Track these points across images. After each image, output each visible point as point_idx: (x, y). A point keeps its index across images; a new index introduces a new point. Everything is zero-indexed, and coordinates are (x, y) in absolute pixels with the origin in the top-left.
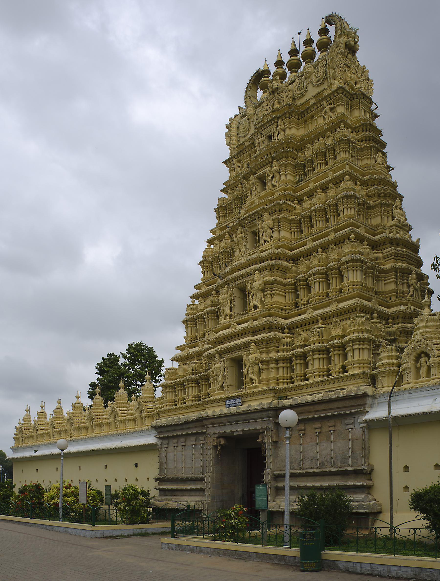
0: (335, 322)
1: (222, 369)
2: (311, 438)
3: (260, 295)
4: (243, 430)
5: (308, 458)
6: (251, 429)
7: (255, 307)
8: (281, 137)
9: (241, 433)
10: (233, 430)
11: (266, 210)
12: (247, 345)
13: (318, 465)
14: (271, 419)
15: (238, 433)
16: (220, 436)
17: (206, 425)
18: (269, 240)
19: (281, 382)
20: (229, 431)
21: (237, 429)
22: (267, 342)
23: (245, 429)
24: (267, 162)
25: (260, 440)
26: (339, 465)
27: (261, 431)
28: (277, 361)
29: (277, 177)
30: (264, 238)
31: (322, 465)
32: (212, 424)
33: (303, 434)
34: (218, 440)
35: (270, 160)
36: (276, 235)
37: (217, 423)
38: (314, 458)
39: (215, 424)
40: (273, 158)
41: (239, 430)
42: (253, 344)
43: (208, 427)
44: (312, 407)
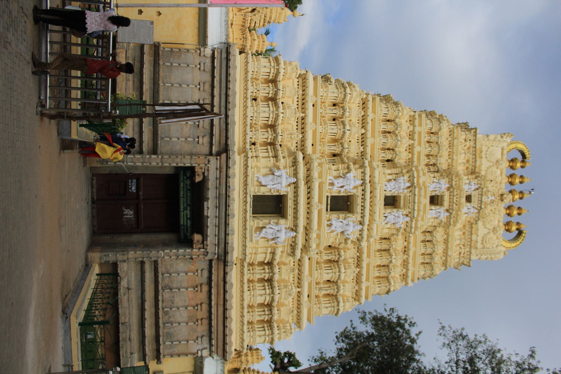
0: (292, 311)
1: (278, 187)
2: (193, 299)
3: (340, 230)
4: (208, 217)
5: (173, 297)
6: (209, 230)
7: (330, 225)
8: (465, 210)
9: (205, 214)
10: (209, 201)
11: (412, 221)
12: (294, 229)
13: (165, 310)
14: (216, 257)
15: (206, 208)
16: (205, 179)
17: (220, 159)
18: (386, 222)
19: (251, 256)
20: (210, 196)
21: (210, 209)
22: (293, 247)
23: (209, 219)
24: (451, 207)
25: (197, 237)
26: (165, 331)
27: (205, 242)
28: (273, 253)
29: (435, 216)
30: (389, 217)
31: (166, 313)
32: (220, 168)
33: (197, 291)
34: (201, 174)
35: (451, 211)
36: (389, 226)
37: (220, 176)
38: (172, 303)
39: (220, 172)
40: (451, 213)
41: (209, 210)
42: (295, 234)
43: (217, 159)
44: (222, 303)
